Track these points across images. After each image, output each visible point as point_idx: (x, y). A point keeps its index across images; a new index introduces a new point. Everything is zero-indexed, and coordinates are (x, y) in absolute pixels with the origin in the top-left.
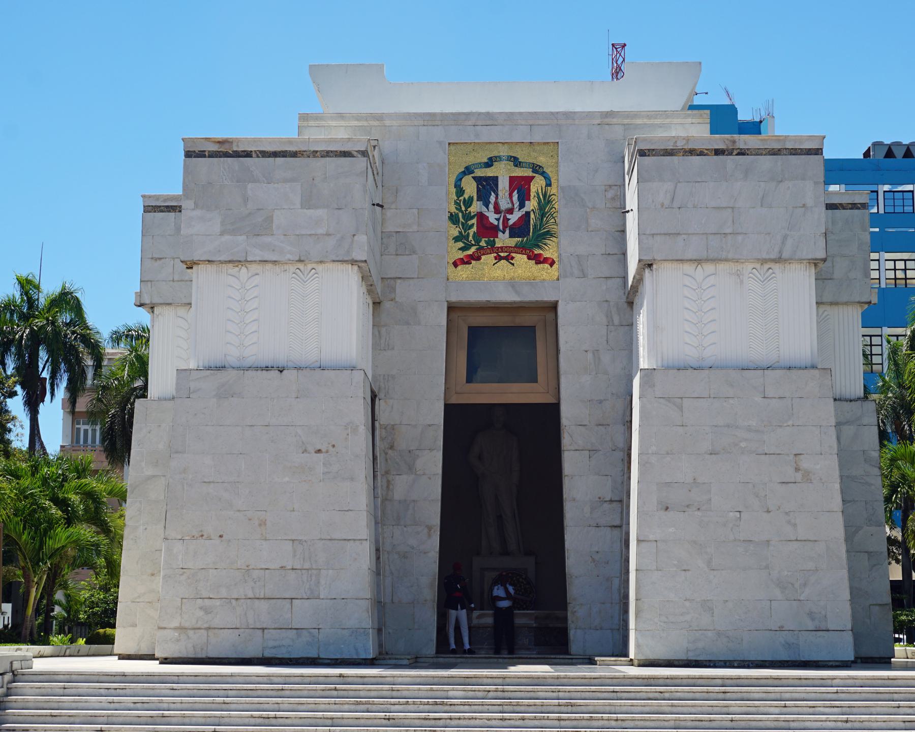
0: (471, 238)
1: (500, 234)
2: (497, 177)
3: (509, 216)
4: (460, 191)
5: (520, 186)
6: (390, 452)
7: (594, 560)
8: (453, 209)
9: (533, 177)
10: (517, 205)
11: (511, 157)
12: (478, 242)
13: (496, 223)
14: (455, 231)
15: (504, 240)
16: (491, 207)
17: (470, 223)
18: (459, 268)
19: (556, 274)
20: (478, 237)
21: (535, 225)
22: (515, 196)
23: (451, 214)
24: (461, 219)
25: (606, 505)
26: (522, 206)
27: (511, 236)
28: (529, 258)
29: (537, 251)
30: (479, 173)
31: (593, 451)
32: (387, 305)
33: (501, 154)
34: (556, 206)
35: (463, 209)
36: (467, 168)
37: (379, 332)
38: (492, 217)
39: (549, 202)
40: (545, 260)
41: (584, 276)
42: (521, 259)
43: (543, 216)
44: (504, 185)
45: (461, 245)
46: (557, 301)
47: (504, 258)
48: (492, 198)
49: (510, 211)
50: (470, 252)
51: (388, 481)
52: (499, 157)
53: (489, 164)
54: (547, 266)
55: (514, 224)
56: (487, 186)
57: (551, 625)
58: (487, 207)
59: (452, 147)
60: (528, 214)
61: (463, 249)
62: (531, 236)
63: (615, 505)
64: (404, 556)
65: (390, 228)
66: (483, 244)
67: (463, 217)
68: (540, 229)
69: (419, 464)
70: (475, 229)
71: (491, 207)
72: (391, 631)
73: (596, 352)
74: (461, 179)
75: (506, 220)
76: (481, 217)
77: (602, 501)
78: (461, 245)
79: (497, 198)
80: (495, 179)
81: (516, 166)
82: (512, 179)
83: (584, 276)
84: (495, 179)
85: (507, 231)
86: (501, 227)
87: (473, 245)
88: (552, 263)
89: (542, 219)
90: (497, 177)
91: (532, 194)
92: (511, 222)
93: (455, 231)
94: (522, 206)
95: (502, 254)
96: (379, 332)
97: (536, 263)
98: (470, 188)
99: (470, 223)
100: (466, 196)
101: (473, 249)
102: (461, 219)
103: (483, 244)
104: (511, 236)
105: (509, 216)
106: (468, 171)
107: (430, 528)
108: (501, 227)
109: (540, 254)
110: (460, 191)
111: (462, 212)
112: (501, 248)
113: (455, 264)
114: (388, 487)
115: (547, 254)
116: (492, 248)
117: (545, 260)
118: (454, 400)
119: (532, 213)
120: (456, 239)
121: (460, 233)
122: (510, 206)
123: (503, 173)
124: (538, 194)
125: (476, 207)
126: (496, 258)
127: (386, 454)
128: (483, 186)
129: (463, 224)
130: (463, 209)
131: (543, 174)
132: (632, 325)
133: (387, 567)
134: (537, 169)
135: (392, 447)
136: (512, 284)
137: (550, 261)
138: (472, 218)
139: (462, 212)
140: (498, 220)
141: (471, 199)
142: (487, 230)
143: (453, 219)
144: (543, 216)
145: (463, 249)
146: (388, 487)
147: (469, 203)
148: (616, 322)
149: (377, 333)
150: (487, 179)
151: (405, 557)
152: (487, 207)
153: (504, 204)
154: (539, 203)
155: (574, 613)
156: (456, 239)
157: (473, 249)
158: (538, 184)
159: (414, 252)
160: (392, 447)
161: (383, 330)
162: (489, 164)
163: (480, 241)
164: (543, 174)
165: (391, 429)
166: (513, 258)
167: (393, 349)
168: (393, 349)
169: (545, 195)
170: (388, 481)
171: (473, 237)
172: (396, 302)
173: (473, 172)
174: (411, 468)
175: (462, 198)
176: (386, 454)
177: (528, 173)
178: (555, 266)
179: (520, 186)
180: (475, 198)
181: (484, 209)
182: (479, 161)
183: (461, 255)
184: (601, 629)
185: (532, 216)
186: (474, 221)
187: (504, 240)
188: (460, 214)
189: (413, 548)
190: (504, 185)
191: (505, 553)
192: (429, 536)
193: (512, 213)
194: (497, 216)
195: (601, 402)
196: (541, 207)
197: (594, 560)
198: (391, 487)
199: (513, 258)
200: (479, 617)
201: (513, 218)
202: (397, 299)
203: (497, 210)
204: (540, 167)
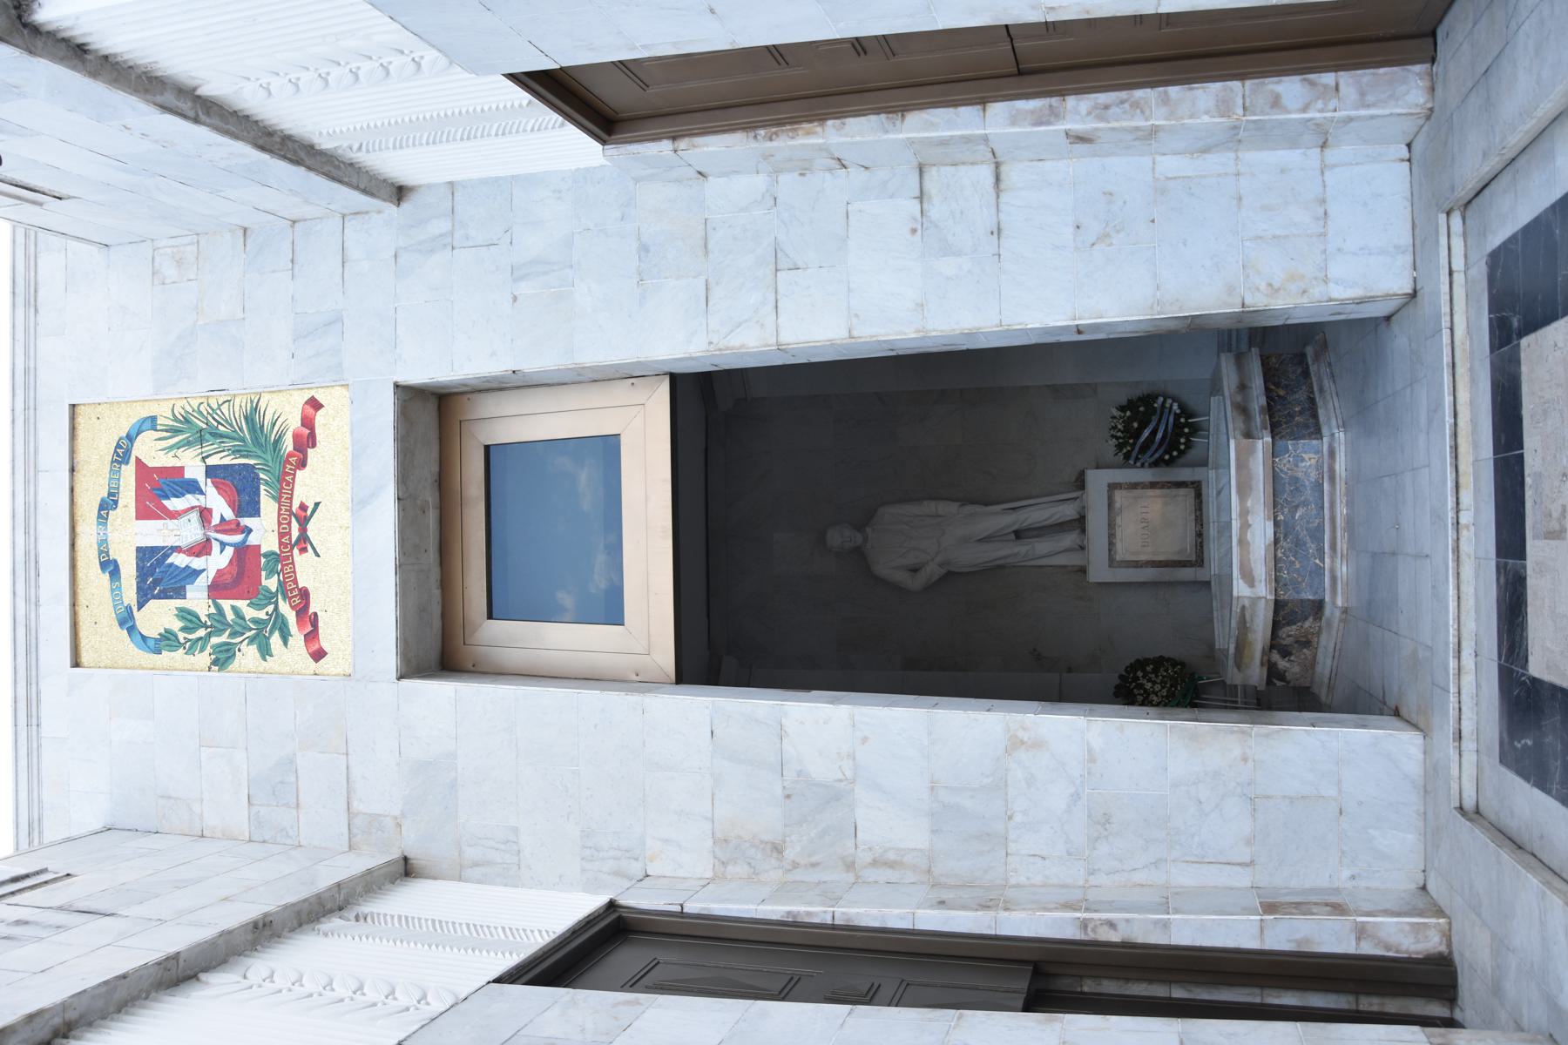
0: (262, 615)
1: (253, 540)
2: (139, 550)
3: (216, 520)
4: (167, 641)
5: (157, 490)
6: (790, 854)
7: (1104, 237)
8: (204, 658)
9: (138, 461)
10: (190, 500)
11: (100, 516)
12: (271, 598)
13: (229, 551)
14: (248, 655)
15: (264, 532)
16: (197, 563)
17: (230, 616)
18: (325, 645)
19: (338, 391)
20: (259, 595)
21: (236, 452)
22: (174, 504)
23: (215, 663)
24: (224, 638)
25: (936, 210)
26: (193, 487)
27: (256, 512)
28: (302, 464)
29: (288, 445)
30: (130, 594)
31: (778, 261)
32: (411, 842)
33: (94, 540)
34: (195, 403)
35: (202, 633)
36: (122, 624)
37: (476, 865)
38: (218, 560)
39: (187, 421)
40: (308, 422)
41: (340, 319)
42: (305, 487)
43: (216, 435)
44: (155, 533)
45: (276, 640)
46: (397, 386)
47: (303, 530)
48: (179, 560)
49: (205, 514)
50: (291, 617)
51: (875, 863)
52: (99, 545)
53: (111, 567)
54: (320, 418)
55: (231, 505)
56: (158, 575)
57: (1263, 401)
58: (197, 573)
59: (85, 657)
60: (211, 471)
61: (285, 638)
62: (259, 465)
63: (931, 186)
64: (1102, 823)
65: (239, 819)
66: (272, 583)
67: (219, 632)
68: (243, 440)
69: (822, 770)
70: (242, 604)
71: (197, 563)
72: (1346, 873)
73: (518, 273)
74: (144, 638)
75: (225, 527)
76: (218, 589)
77: (921, 225)
78: (276, 640)
79: (178, 549)
80: (144, 553)
81: (116, 502)
82: (143, 513)
83: (336, 321)
84: (144, 553)
85: (246, 521)
86: (238, 538)
87: (276, 609)
88: (315, 404)
89: (221, 436)
90: (139, 550)
91: (167, 461)
92: (229, 514)
93: (248, 655)
94: (193, 487)
95: (295, 534)
96: (476, 865)
97: (314, 445)
98: (159, 616)
99: (230, 616)
100: (176, 625)
101: (285, 608)
102: (224, 638)
103: (272, 583)
104: (256, 512)
105: (216, 520)
106: (126, 621)
107: (1015, 744)
108: (238, 538)
109: (296, 437)
110: (167, 641)
111: (209, 635)
112: (281, 535)
113: (319, 655)
114: (892, 865)
115: (294, 422)
116: (281, 560)
117: (308, 422)
118: (665, 657)
119: (210, 462)
120: (265, 652)
121: (252, 640)
122: (194, 516)
123: (131, 534)
124: (171, 448)
125: (197, 599)
126: (303, 550)
127: (795, 865)
128: (156, 582)
129: (234, 634)
130: (202, 633)
131: (130, 438)
132: (451, 184)
133: (1138, 877)
134: (122, 454)
135: (777, 849)
136: (359, 504)
137: (310, 411)
138: (218, 607)
139: (209, 635)
140: (223, 545)
141: (184, 614)
142: (242, 576)
143: (223, 658)
144: (216, 435)
145: (285, 638)
146: (892, 865)
147: (188, 616)
148: (442, 226)
149: (478, 872)
150: (142, 574)
151: (1106, 820)
152: (197, 573)
153: (188, 531)
154: (188, 444)
155: (1274, 290)
156: (265, 652)
157: (285, 608)
158: (151, 451)
159: (291, 761)
160: (777, 849)
161: (471, 853)
162: (111, 567)
163: (268, 590)
164: (130, 438)
165: (726, 847)
166: (303, 507)
167: (515, 830)
168: (515, 830)
169: (175, 431)
170: (875, 863)
171: (259, 607)
172: (403, 815)
173: (129, 609)
174: (835, 795)
175: (181, 636)
176: (795, 865)
177: (129, 472)
178: (320, 398)
179: (157, 490)
180: (179, 603)
181: (203, 581)
182: (108, 594)
183: (297, 639)
184: (1323, 201)
185: (214, 461)
186: (226, 605)
187: (264, 532)
188: (215, 640)
189: (1076, 796)
190: (155, 533)
191: (1080, 523)
192: (1038, 745)
193: (210, 511)
194: (216, 547)
195: (644, 248)
196: (200, 438)
197: (1104, 237)
198: (891, 856)
199: (303, 507)
200: (1250, 580)
201: (221, 508)
202: (397, 813)
203: (202, 549)
204: (118, 446)
